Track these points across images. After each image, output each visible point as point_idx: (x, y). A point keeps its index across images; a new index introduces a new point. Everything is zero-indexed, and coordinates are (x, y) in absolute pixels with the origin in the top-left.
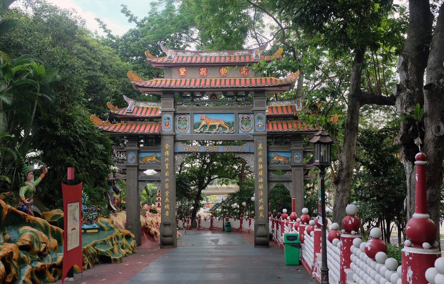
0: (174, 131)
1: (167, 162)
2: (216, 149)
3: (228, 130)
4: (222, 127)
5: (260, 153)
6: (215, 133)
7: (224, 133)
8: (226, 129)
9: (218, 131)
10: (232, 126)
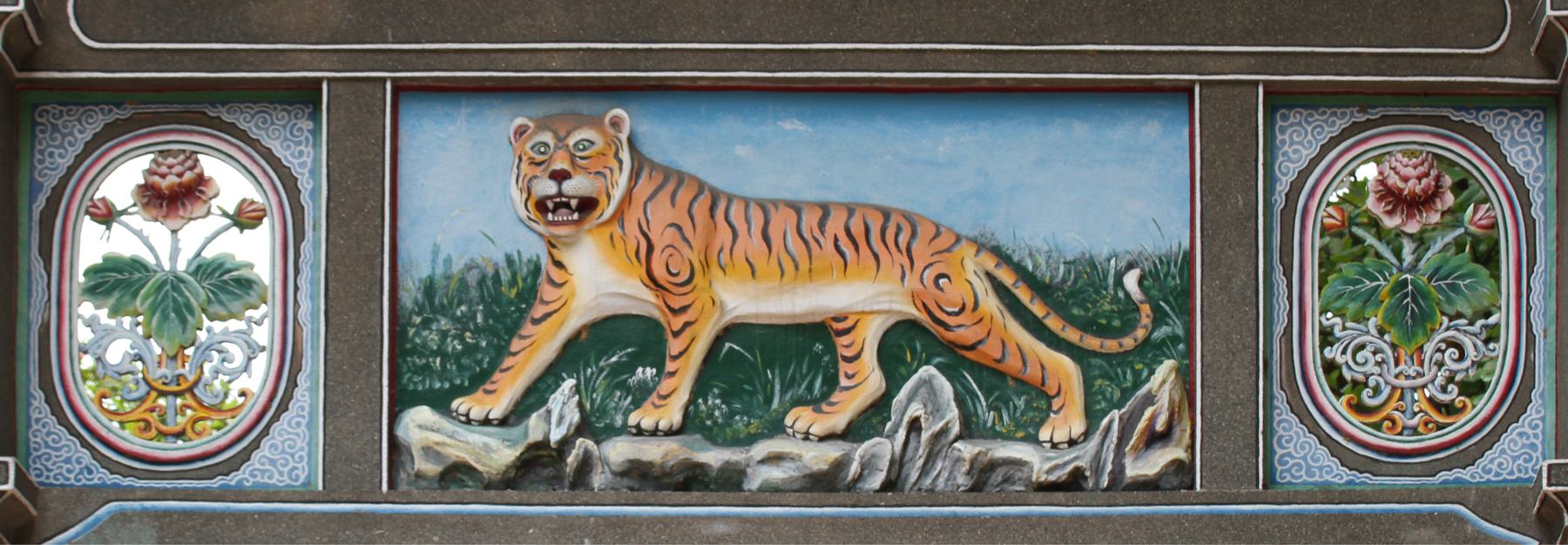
3: (1067, 422)
4: (956, 359)
6: (825, 483)
7: (984, 477)
8: (1041, 398)
9: (884, 448)
10: (1151, 351)
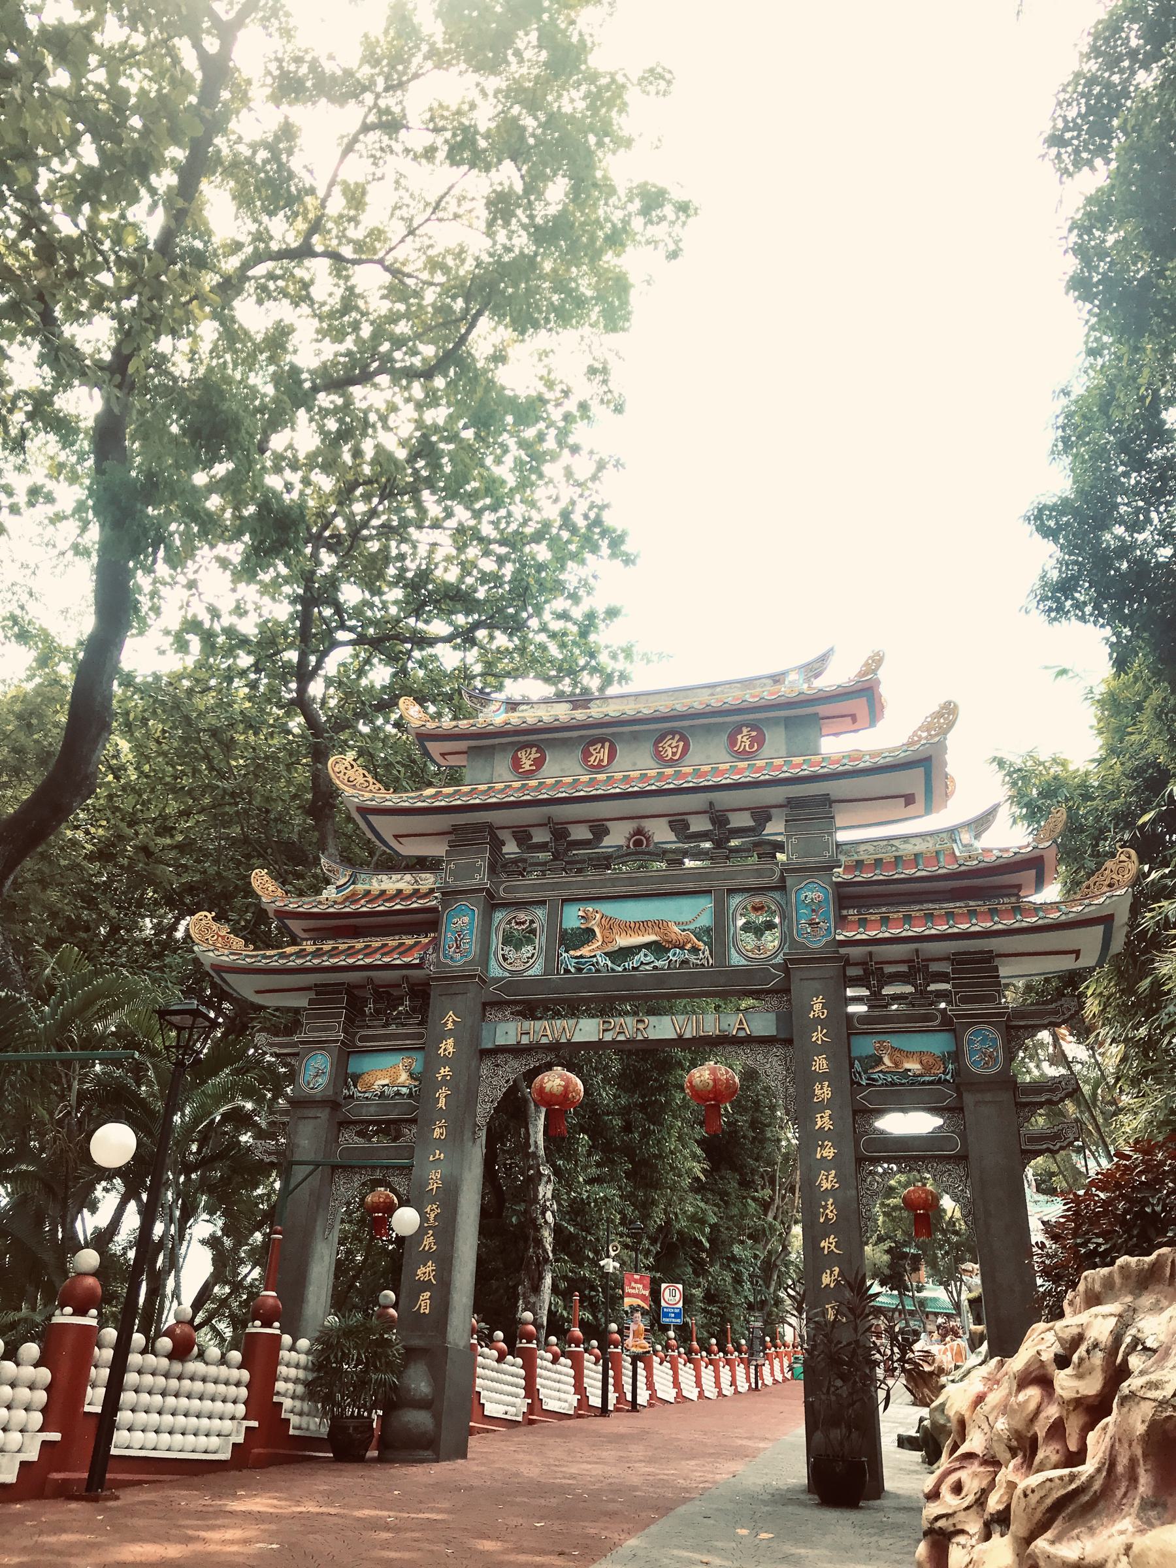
0: (485, 963)
1: (444, 1082)
2: (641, 1026)
5: (818, 1036)
